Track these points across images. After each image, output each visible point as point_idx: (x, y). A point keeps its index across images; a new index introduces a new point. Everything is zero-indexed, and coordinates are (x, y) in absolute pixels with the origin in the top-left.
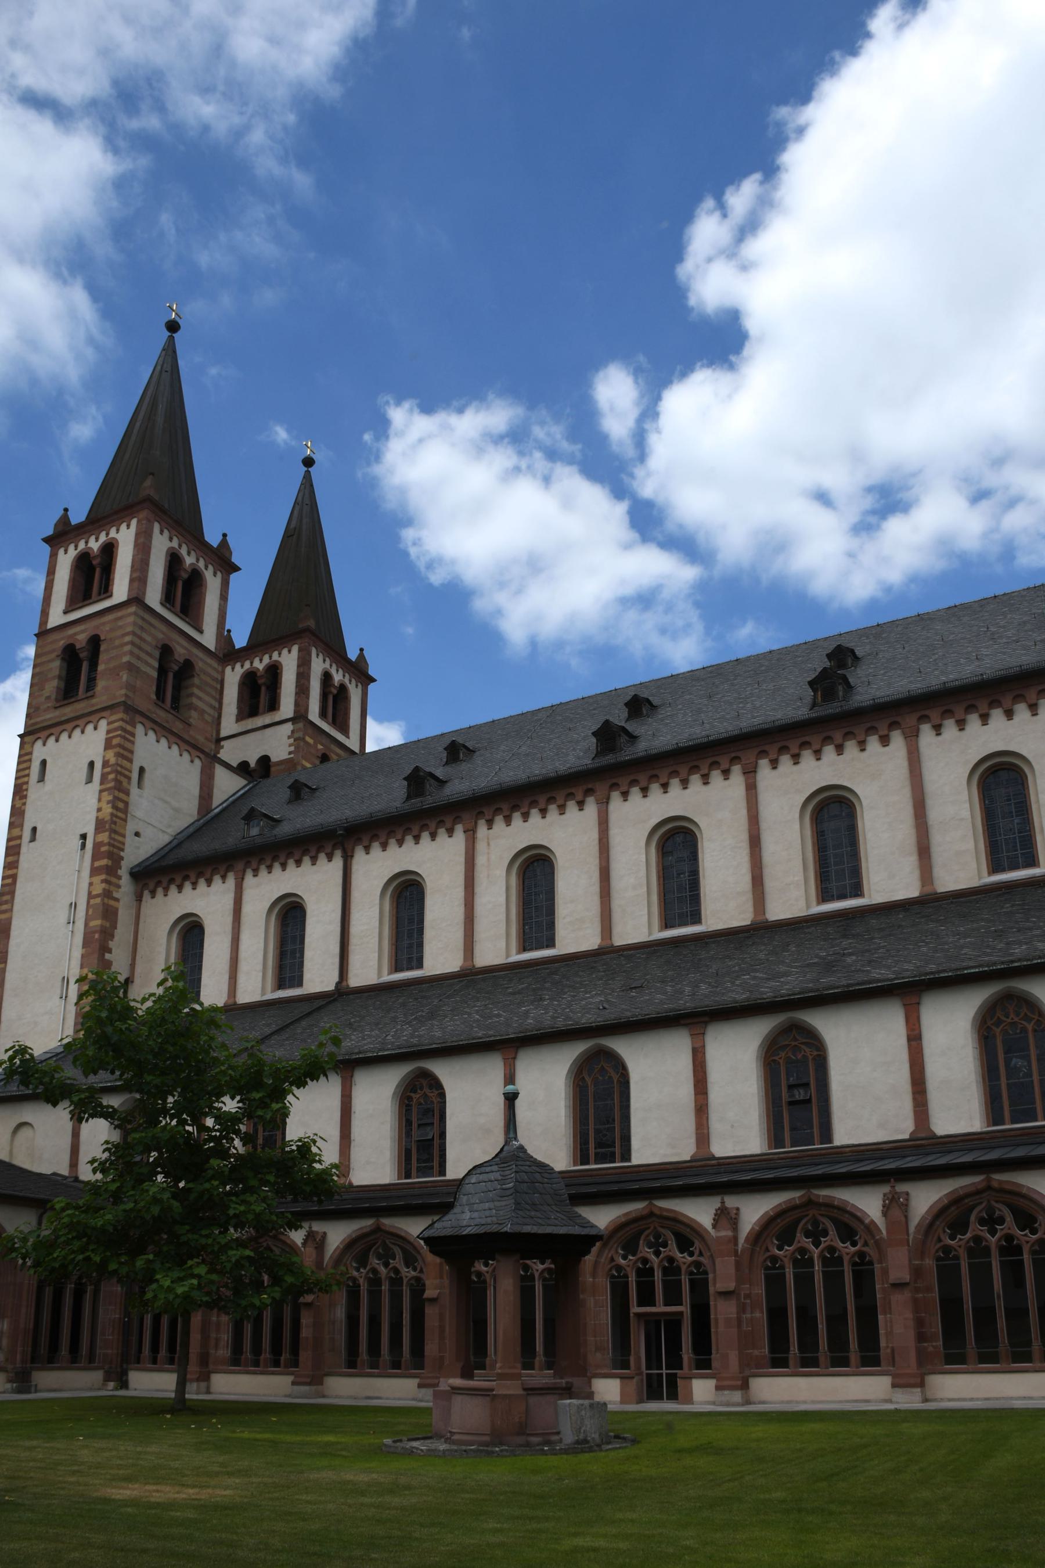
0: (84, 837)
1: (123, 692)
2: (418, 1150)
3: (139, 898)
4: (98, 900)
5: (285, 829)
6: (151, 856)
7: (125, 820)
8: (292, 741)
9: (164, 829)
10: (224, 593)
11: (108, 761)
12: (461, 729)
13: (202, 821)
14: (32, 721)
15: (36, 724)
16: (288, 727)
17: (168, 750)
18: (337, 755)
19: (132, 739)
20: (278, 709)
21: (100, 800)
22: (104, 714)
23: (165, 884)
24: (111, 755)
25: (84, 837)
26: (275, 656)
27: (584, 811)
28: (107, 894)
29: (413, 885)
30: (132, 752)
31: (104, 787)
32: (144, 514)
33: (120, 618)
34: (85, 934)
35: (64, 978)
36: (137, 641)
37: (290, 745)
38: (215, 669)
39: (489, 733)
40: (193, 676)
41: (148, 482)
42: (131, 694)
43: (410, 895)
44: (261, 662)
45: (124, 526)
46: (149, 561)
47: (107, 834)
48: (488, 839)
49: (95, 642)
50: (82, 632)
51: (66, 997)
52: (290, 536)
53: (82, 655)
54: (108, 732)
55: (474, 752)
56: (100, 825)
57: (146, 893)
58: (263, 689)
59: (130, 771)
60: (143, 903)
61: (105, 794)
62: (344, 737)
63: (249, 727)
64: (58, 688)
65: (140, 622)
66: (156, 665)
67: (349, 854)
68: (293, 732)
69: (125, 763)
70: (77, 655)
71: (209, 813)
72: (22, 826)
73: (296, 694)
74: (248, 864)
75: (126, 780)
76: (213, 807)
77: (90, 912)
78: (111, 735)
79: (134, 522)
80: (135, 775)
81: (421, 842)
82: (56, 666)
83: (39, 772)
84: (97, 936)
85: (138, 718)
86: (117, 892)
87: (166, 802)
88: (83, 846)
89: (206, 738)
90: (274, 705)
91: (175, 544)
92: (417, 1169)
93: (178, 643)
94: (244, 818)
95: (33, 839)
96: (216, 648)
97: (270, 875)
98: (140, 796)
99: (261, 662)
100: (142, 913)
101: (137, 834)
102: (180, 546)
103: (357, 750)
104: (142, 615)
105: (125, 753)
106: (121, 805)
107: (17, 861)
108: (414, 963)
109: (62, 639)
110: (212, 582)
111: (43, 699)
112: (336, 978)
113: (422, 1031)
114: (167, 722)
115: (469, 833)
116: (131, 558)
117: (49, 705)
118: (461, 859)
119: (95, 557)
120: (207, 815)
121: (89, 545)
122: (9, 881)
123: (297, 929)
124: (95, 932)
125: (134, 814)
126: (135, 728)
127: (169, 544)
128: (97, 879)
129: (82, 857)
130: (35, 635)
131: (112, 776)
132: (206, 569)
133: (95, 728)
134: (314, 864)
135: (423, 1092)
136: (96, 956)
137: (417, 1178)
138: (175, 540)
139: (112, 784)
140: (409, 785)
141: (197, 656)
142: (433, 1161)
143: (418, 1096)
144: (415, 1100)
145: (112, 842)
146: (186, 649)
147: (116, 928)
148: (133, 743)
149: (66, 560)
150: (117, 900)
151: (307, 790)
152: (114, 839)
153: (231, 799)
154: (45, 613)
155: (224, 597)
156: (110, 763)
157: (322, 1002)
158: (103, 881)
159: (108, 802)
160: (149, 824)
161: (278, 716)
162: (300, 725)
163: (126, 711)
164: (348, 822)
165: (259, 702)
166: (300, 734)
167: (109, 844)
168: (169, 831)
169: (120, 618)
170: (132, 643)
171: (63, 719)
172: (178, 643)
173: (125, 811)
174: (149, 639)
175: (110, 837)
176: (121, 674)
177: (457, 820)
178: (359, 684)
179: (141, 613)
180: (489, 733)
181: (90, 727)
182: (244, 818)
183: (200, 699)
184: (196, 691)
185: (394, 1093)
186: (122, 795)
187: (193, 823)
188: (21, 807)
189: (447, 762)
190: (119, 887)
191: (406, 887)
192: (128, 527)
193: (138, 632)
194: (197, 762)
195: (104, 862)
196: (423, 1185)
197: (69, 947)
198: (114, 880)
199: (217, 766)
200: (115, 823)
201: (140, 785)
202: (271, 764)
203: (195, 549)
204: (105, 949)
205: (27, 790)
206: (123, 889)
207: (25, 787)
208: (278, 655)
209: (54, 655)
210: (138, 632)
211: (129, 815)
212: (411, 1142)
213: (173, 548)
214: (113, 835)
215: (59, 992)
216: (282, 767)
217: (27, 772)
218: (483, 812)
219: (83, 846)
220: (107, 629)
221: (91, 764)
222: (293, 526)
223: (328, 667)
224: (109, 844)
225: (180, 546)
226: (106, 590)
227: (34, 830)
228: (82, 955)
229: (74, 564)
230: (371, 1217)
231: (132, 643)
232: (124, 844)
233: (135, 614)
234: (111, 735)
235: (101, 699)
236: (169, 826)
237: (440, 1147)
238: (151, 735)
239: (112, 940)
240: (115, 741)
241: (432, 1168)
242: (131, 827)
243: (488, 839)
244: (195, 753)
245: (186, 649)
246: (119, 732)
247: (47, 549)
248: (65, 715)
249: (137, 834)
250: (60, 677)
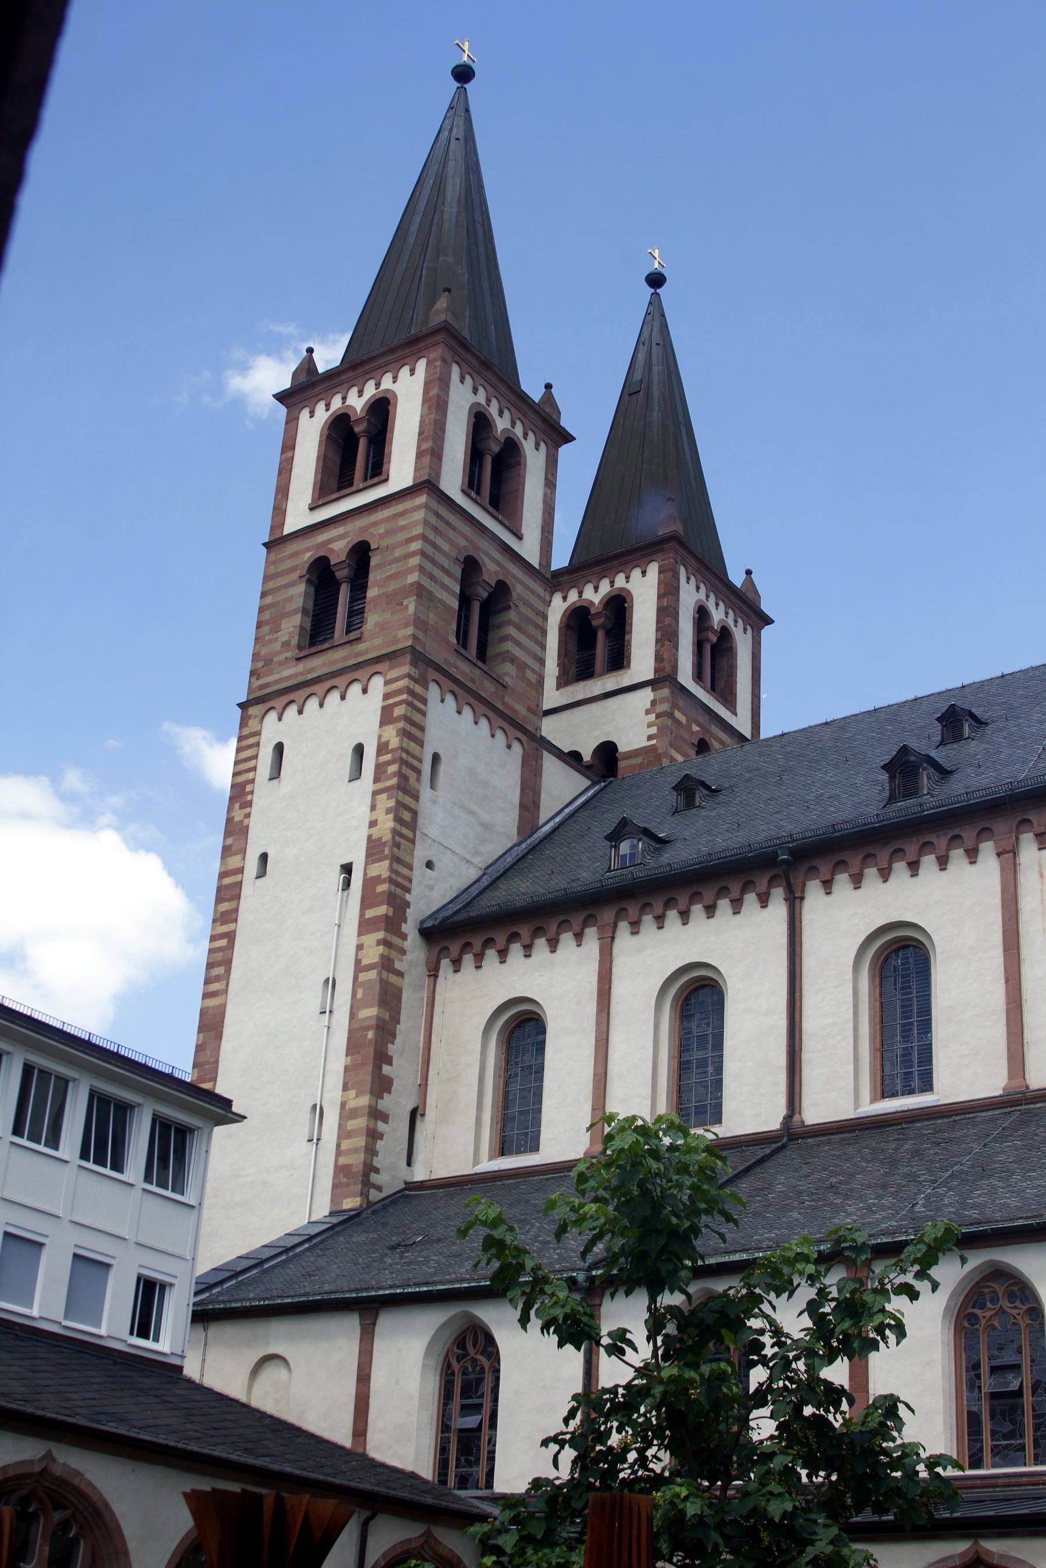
0: (347, 869)
1: (410, 630)
2: (992, 1416)
3: (433, 972)
4: (373, 974)
5: (676, 857)
6: (451, 902)
7: (413, 842)
8: (652, 717)
9: (468, 857)
10: (550, 477)
11: (387, 743)
12: (948, 691)
13: (524, 846)
14: (261, 682)
15: (266, 685)
16: (646, 695)
17: (474, 725)
18: (722, 742)
19: (422, 706)
20: (628, 666)
21: (373, 808)
22: (378, 667)
23: (477, 948)
24: (391, 735)
25: (347, 869)
26: (620, 581)
27: (947, 871)
28: (386, 964)
29: (908, 946)
30: (422, 729)
31: (380, 786)
32: (436, 353)
33: (403, 514)
34: (351, 1032)
35: (315, 1106)
36: (429, 550)
37: (650, 725)
38: (538, 596)
39: (1000, 695)
40: (509, 607)
41: (442, 303)
42: (420, 635)
43: (902, 964)
44: (596, 591)
45: (405, 371)
46: (445, 424)
47: (387, 863)
48: (1040, 866)
49: (361, 553)
51: (318, 1140)
52: (631, 391)
53: (341, 574)
54: (386, 696)
55: (987, 724)
57: (445, 964)
58: (601, 635)
59: (420, 761)
60: (617, 942)
62: (728, 713)
63: (580, 697)
64: (302, 628)
65: (433, 520)
66: (457, 589)
67: (798, 895)
68: (653, 703)
69: (412, 746)
70: (332, 573)
71: (535, 832)
72: (243, 851)
73: (657, 641)
74: (621, 915)
75: (415, 774)
76: (541, 823)
77: (360, 995)
78: (391, 701)
79: (421, 365)
80: (426, 767)
81: (921, 871)
82: (298, 593)
83: (272, 763)
84: (370, 1035)
85: (432, 674)
86: (401, 960)
87: (473, 813)
88: (347, 884)
89: (529, 709)
90: (619, 660)
91: (481, 397)
92: (992, 1451)
93: (489, 556)
94: (609, 838)
95: (262, 873)
96: (540, 564)
97: (662, 931)
98: (434, 802)
99: (596, 591)
100: (437, 997)
101: (429, 865)
102: (488, 401)
103: (748, 734)
104: (436, 509)
105: (414, 731)
106: (407, 816)
107: (236, 910)
108: (916, 1083)
109: (307, 550)
110: (534, 458)
111: (277, 646)
112: (782, 1111)
113: (979, 1196)
114: (473, 681)
115: (1006, 855)
116: (418, 419)
117: (289, 655)
118: (995, 901)
119: (359, 420)
120: (531, 835)
121: (349, 402)
122: (223, 943)
123: (709, 1023)
124: (368, 1028)
125: (425, 831)
126: (427, 689)
127: (473, 399)
128: (371, 939)
129: (344, 904)
130: (264, 545)
131: (393, 768)
132: (526, 439)
133: (365, 691)
134: (736, 912)
135: (998, 1306)
136: (370, 1069)
137: (994, 1466)
138: (481, 391)
139: (394, 781)
140: (892, 778)
141: (515, 577)
142: (1022, 1436)
143: (988, 1314)
144: (983, 1322)
145: (394, 876)
146: (498, 564)
147: (398, 1022)
148: (424, 714)
150: (400, 974)
151: (705, 792)
152: (397, 873)
153: (567, 811)
154: (279, 512)
155: (550, 483)
156: (390, 748)
157: (760, 1152)
158: (379, 942)
159: (388, 811)
160: (446, 847)
161: (626, 678)
162: (665, 692)
163: (414, 663)
164: (794, 841)
165: (593, 657)
166: (664, 707)
167: (391, 880)
168: (476, 860)
169: (403, 514)
170: (423, 553)
171: (310, 676)
172: (489, 556)
173: (413, 826)
174: (445, 546)
175: (392, 870)
176: (405, 602)
177: (985, 833)
178: (749, 628)
179: (434, 505)
180: (1000, 695)
181: (356, 689)
182: (609, 838)
183: (518, 644)
184: (511, 630)
185: (947, 1308)
186: (408, 800)
187: (511, 849)
188: (242, 821)
189: (942, 740)
190: (403, 952)
191: (897, 950)
192: (412, 372)
193: (431, 536)
194: (517, 748)
195: (382, 910)
196: (1013, 1480)
197: (323, 1054)
198: (396, 940)
199: (545, 754)
200: (398, 845)
201: (433, 786)
202: (617, 755)
203: (510, 406)
204: (382, 1058)
205: (252, 792)
206: (409, 957)
207: (248, 788)
208: (624, 580)
209: (295, 575)
210: (431, 536)
211: (418, 833)
212: (980, 1399)
213: (478, 404)
214: (395, 866)
215: (306, 1130)
216: (638, 760)
217: (252, 764)
218: (1028, 821)
219: (347, 884)
220: (382, 531)
221: (359, 750)
222: (638, 375)
223: (703, 598)
224: (391, 880)
225: (488, 401)
226: (377, 470)
227: (264, 858)
228: (346, 1067)
229: (326, 432)
230: (964, 1537)
231: (423, 553)
232: (410, 881)
233: (426, 506)
234: (391, 701)
235: (372, 645)
236: (476, 853)
237: (1034, 1410)
238: (450, 699)
239: (393, 1043)
240: (398, 711)
241: (1022, 1448)
242: (421, 853)
243: (1040, 866)
244: (513, 732)
245: (498, 564)
246: (404, 696)
247: (282, 411)
249: (429, 865)
250: (304, 611)
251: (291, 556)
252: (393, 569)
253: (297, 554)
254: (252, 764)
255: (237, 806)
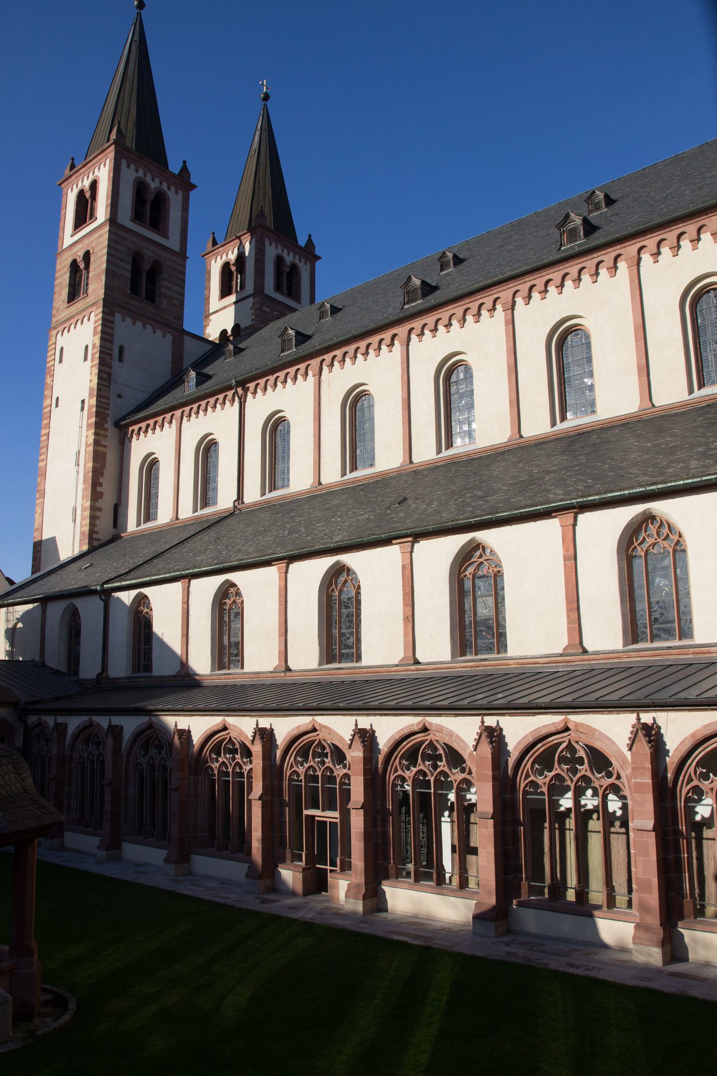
7: (109, 387)
21: (91, 374)
30: (112, 335)
61: (94, 368)
66: (130, 268)
75: (108, 357)
77: (87, 458)
91: (141, 174)
96: (180, 250)
101: (119, 396)
102: (145, 175)
126: (114, 317)
127: (135, 175)
148: (112, 328)
150: (106, 447)
178: (308, 262)
211: (112, 383)
225: (145, 175)
234: (97, 324)
238: (128, 319)
239: (102, 477)
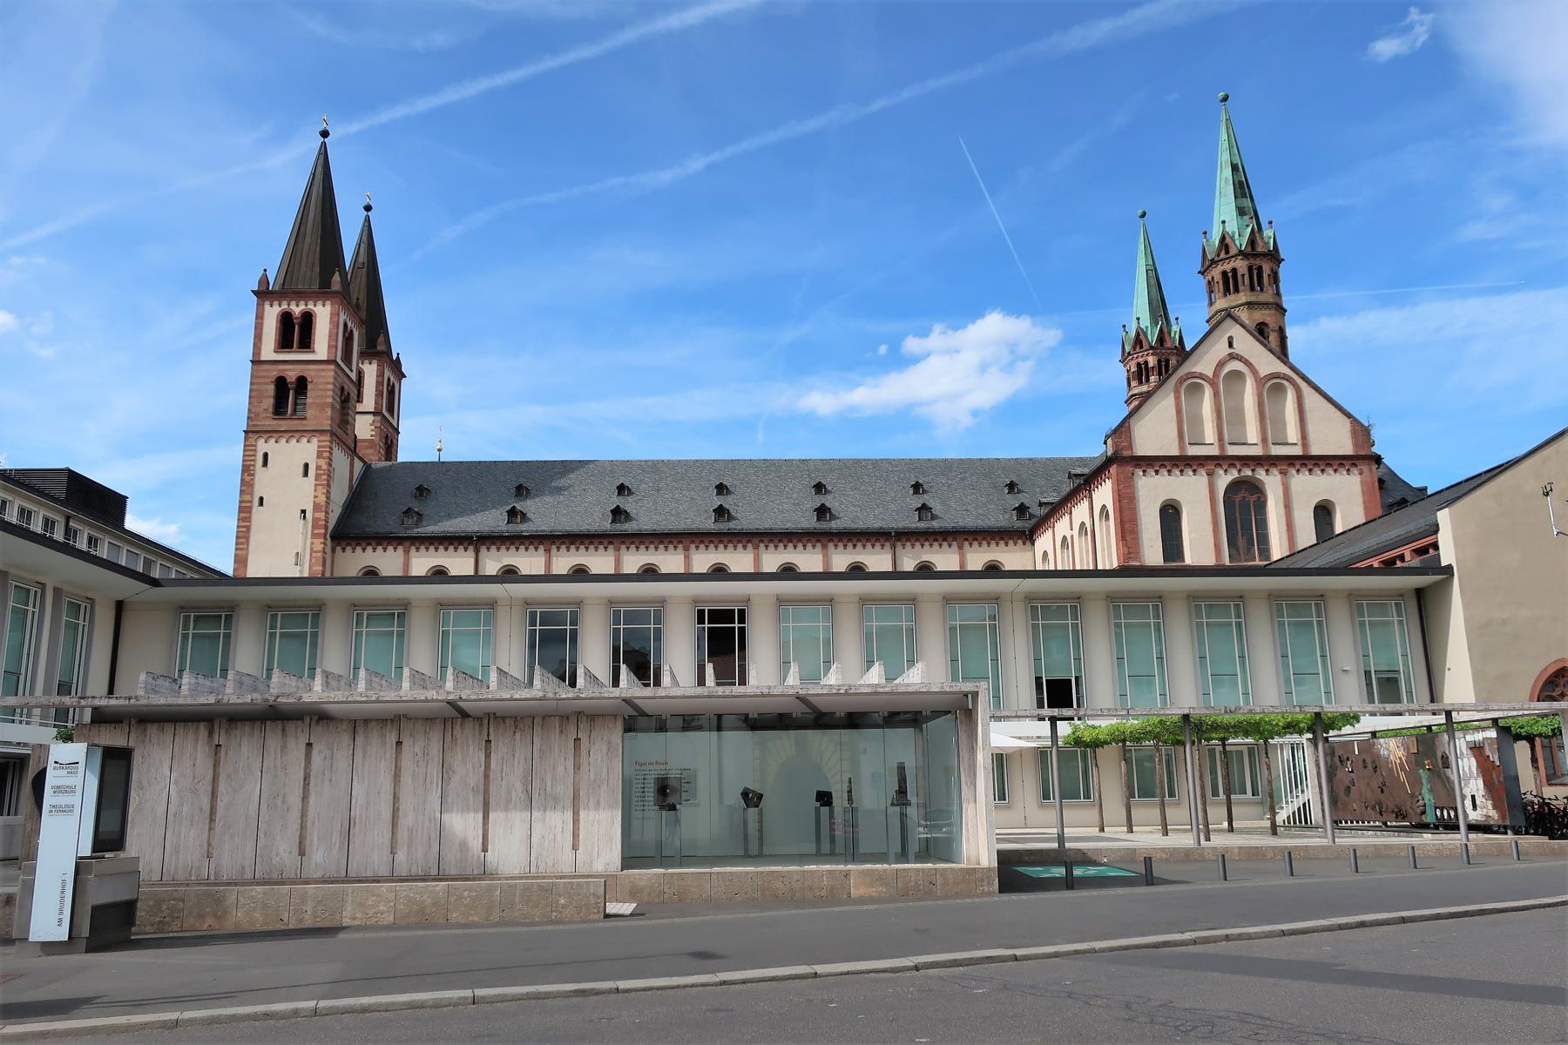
0: (304, 512)
21: (315, 490)
22: (314, 434)
25: (304, 512)
33: (323, 370)
50: (293, 370)
56: (316, 507)
77: (313, 561)
149: (272, 313)
169: (323, 370)
248: (280, 425)
251: (265, 370)
252: (320, 393)
253: (268, 370)
254: (253, 458)
255: (246, 474)
